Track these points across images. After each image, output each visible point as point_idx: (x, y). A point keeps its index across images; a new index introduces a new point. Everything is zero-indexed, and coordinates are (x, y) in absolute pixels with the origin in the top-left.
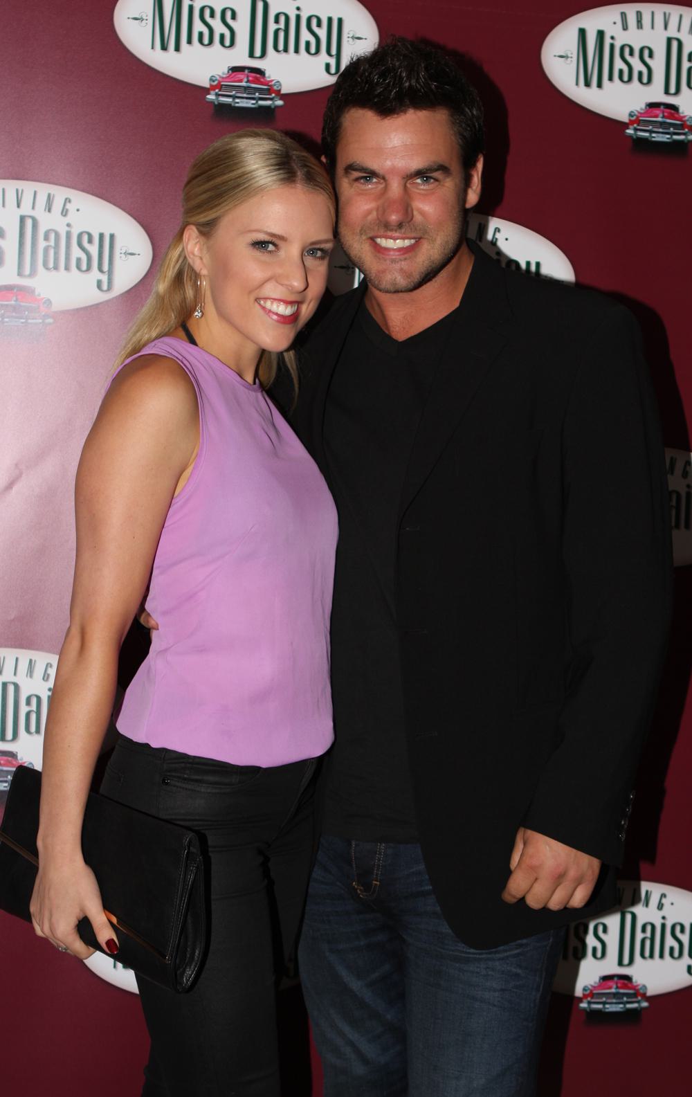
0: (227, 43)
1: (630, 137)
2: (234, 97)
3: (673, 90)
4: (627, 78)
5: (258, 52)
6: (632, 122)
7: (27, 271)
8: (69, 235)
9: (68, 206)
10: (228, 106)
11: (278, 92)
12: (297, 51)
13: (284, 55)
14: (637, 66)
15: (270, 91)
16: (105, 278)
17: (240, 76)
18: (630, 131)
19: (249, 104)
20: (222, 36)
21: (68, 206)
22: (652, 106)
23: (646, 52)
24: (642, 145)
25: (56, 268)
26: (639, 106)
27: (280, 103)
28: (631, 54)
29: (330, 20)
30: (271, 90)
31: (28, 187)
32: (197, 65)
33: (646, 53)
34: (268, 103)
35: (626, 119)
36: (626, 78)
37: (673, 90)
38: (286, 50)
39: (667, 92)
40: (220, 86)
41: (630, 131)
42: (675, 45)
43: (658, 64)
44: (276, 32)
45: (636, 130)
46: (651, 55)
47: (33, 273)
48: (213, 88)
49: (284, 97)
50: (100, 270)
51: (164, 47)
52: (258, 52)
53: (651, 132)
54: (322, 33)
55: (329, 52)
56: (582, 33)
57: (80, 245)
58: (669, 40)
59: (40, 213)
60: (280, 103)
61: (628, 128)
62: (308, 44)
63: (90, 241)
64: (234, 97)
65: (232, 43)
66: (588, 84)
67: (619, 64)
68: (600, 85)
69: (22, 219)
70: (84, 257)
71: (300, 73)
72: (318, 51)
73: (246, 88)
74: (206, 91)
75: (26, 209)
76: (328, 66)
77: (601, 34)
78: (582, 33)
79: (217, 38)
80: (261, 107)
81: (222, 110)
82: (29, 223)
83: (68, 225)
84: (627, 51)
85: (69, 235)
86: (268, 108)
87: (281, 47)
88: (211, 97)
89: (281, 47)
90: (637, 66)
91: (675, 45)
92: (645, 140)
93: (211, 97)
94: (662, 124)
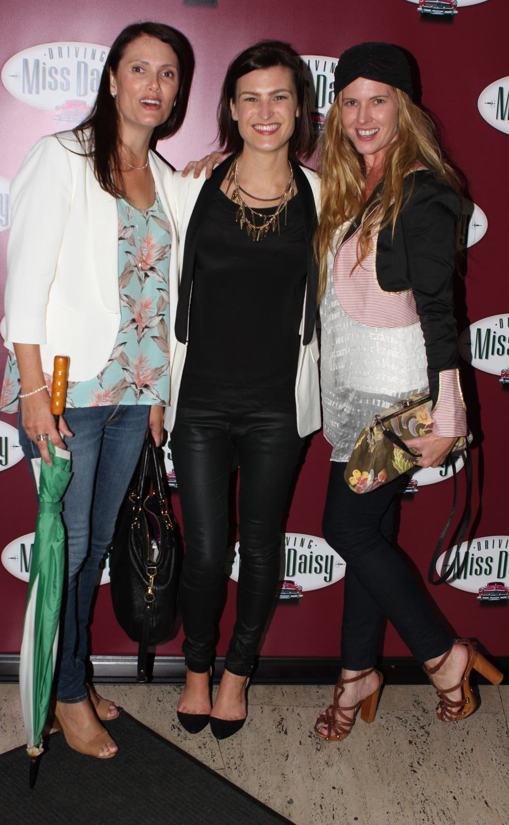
1: (420, 12)
7: (82, 92)
18: (420, 9)
31: (81, 46)
41: (420, 9)
47: (86, 94)
53: (432, 9)
59: (88, 60)
69: (79, 64)
75: (81, 58)
82: (83, 66)
92: (428, 14)
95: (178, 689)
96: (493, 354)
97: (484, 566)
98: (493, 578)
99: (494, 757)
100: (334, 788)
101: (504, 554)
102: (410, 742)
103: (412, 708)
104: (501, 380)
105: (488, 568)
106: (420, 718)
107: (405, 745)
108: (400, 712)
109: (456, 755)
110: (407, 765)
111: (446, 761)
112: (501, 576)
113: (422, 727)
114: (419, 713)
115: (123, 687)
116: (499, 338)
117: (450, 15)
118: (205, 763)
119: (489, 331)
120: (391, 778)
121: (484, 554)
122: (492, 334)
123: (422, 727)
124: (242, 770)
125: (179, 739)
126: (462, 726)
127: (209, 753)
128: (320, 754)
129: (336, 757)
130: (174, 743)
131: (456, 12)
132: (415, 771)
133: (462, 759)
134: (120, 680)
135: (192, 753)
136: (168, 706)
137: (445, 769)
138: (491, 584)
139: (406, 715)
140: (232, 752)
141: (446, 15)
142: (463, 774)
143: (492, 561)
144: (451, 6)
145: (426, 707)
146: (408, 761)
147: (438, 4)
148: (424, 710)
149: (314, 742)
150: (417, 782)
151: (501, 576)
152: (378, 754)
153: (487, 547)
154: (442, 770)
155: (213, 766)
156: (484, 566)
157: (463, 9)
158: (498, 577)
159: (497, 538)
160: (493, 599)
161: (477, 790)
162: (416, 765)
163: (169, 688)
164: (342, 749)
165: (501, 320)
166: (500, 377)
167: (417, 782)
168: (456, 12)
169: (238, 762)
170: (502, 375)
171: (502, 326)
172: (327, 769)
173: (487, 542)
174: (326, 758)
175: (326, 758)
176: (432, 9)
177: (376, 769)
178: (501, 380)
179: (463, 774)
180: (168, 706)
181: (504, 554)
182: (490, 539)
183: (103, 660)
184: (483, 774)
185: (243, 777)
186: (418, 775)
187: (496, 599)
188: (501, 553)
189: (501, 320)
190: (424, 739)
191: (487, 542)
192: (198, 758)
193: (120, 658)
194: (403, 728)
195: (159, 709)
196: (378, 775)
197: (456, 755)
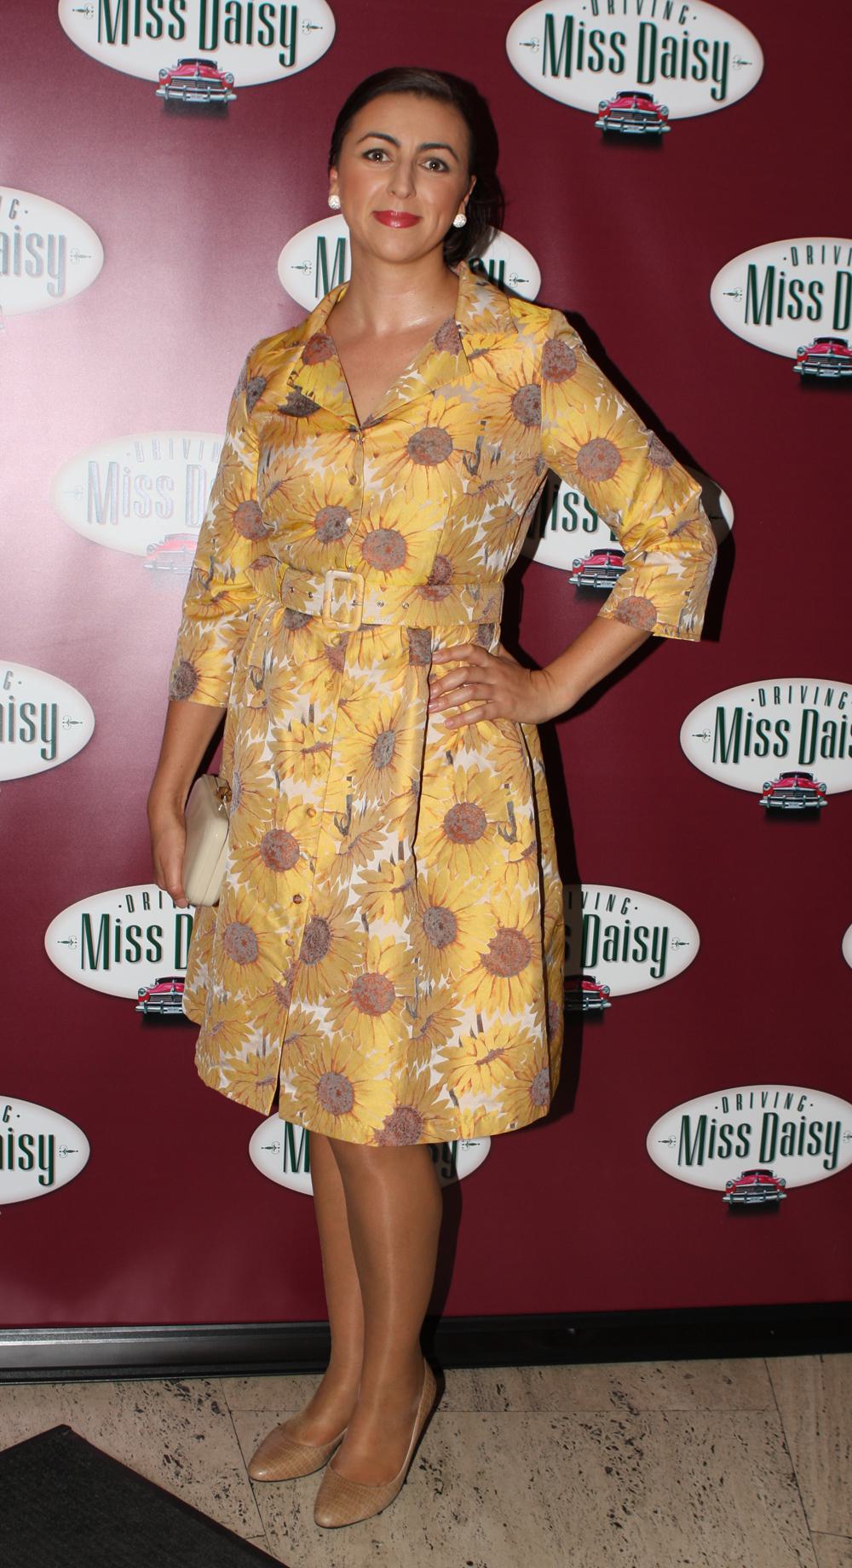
0: (177, 34)
2: (185, 91)
3: (646, 78)
4: (597, 66)
5: (209, 44)
6: (602, 114)
8: (18, 237)
9: (16, 208)
10: (180, 100)
11: (230, 86)
12: (249, 41)
13: (236, 46)
14: (608, 53)
15: (222, 84)
16: (56, 282)
17: (191, 69)
18: (600, 123)
19: (201, 98)
20: (171, 28)
21: (16, 208)
22: (624, 95)
23: (618, 39)
24: (612, 136)
25: (6, 272)
26: (610, 96)
27: (232, 97)
28: (602, 40)
29: (284, 9)
30: (223, 84)
32: (146, 59)
33: (618, 39)
34: (221, 97)
35: (596, 110)
36: (596, 66)
37: (646, 78)
38: (238, 41)
39: (640, 80)
40: (170, 80)
41: (600, 123)
42: (648, 30)
43: (631, 51)
44: (228, 22)
45: (606, 121)
46: (623, 41)
48: (163, 82)
49: (237, 90)
50: (51, 274)
51: (111, 40)
52: (209, 44)
53: (623, 123)
54: (276, 23)
55: (283, 43)
56: (550, 19)
57: (29, 248)
58: (643, 26)
60: (232, 97)
62: (261, 34)
63: (40, 244)
64: (185, 91)
65: (182, 35)
66: (555, 73)
67: (589, 52)
68: (568, 74)
70: (33, 260)
71: (250, 65)
72: (271, 41)
73: (197, 82)
74: (157, 85)
76: (282, 58)
77: (569, 21)
78: (550, 19)
79: (166, 30)
80: (212, 102)
81: (173, 106)
83: (17, 228)
84: (597, 37)
85: (18, 237)
86: (219, 104)
87: (233, 37)
88: (161, 91)
89: (233, 37)
90: (608, 53)
91: (648, 30)
92: (616, 132)
93: (161, 91)
94: (634, 115)
95: (174, 1387)
96: (747, 753)
97: (735, 1140)
98: (752, 1162)
99: (762, 1492)
100: (470, 1563)
101: (771, 1118)
102: (608, 1471)
103: (609, 1406)
105: (742, 1145)
106: (627, 1425)
107: (598, 1478)
108: (588, 1416)
109: (693, 1491)
110: (603, 1514)
111: (675, 1502)
112: (767, 1157)
113: (629, 1442)
114: (622, 1416)
115: (69, 1387)
116: (759, 724)
117: (654, 134)
118: (228, 1526)
119: (739, 711)
120: (575, 1540)
121: (735, 1118)
122: (745, 718)
123: (629, 1442)
124: (297, 1536)
125: (178, 1481)
126: (701, 1437)
127: (236, 1507)
128: (442, 1501)
129: (472, 1505)
130: (170, 1489)
131: (666, 128)
132: (618, 1525)
133: (703, 1498)
134: (64, 1374)
135: (202, 1508)
136: (156, 1419)
137: (674, 1519)
138: (748, 1174)
139: (599, 1420)
140: (278, 1502)
142: (706, 1526)
143: (748, 1131)
144: (657, 117)
145: (634, 1403)
146: (606, 1507)
148: (631, 1410)
149: (431, 1478)
150: (624, 1546)
151: (767, 1157)
152: (549, 1496)
153: (739, 1106)
154: (668, 1520)
155: (243, 1531)
156: (735, 1140)
158: (762, 1160)
159: (758, 1090)
160: (751, 1200)
161: (733, 1555)
162: (620, 1513)
163: (157, 1385)
164: (482, 1490)
165: (762, 692)
167: (624, 1546)
168: (666, 128)
169: (290, 1521)
170: (766, 793)
171: (763, 703)
172: (456, 1528)
173: (739, 1097)
174: (454, 1507)
175: (454, 1507)
177: (546, 1524)
179: (706, 1526)
180: (156, 1419)
181: (771, 1118)
182: (745, 1092)
183: (32, 1338)
184: (744, 1526)
185: (301, 1550)
186: (625, 1532)
187: (759, 1200)
188: (766, 1116)
189: (762, 692)
190: (633, 1463)
191: (739, 1097)
192: (215, 1517)
193: (63, 1332)
194: (595, 1445)
195: (140, 1427)
196: (551, 1534)
197: (693, 1491)
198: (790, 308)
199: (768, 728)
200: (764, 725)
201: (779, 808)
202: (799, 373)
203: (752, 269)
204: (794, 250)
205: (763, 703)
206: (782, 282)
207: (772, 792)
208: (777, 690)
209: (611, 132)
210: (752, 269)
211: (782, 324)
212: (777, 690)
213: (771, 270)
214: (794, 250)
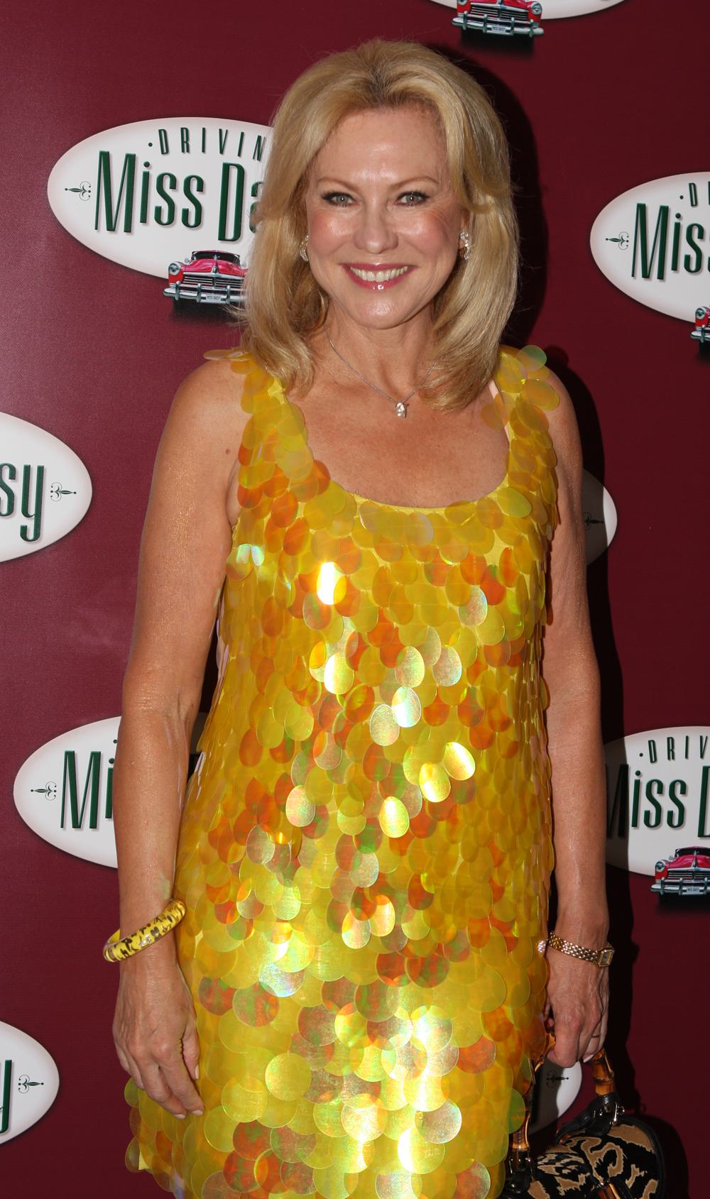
18: (459, 20)
41: (459, 20)
45: (466, 18)
53: (486, 22)
61: (456, 16)
104: (656, 886)
116: (649, 785)
117: (525, 36)
131: (539, 31)
141: (517, 35)
144: (527, 15)
147: (500, 12)
157: (558, 26)
165: (652, 745)
166: (651, 880)
168: (539, 31)
170: (658, 875)
171: (653, 759)
176: (486, 22)
178: (656, 886)
189: (652, 745)
198: (688, 258)
199: (660, 791)
200: (655, 787)
201: (675, 895)
202: (697, 340)
203: (642, 209)
204: (692, 187)
205: (653, 759)
206: (678, 226)
207: (666, 873)
208: (671, 742)
209: (472, 32)
210: (642, 209)
211: (678, 279)
212: (671, 742)
213: (664, 211)
214: (692, 187)
